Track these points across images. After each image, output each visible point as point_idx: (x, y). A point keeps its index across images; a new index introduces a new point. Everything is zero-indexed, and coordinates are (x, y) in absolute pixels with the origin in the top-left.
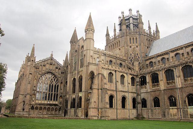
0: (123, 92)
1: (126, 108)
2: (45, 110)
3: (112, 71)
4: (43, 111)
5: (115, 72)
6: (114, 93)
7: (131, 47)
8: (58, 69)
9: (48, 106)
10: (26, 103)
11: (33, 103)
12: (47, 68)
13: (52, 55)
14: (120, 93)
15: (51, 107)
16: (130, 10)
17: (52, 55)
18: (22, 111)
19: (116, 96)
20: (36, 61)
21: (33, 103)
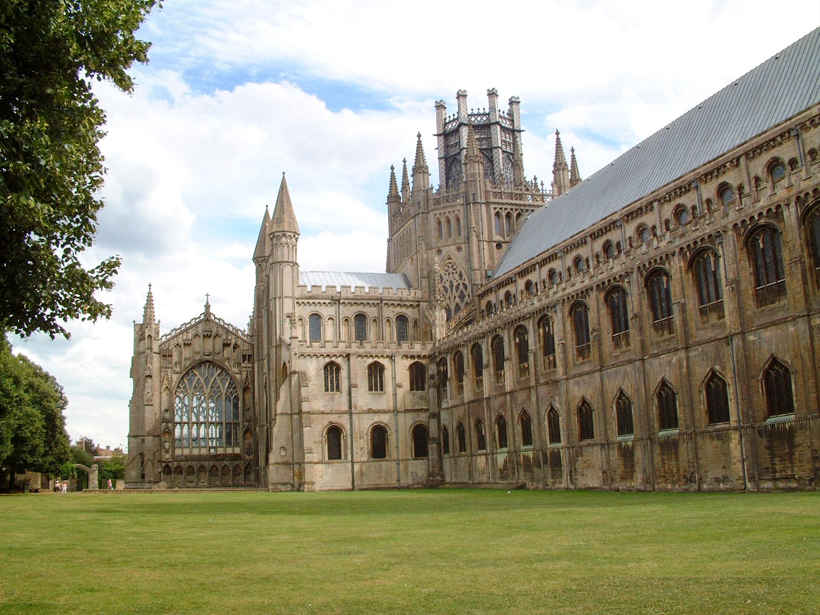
0: (378, 412)
1: (387, 458)
2: (202, 475)
3: (334, 359)
4: (198, 477)
5: (346, 359)
6: (344, 421)
7: (439, 252)
8: (232, 346)
9: (212, 463)
10: (146, 458)
11: (167, 456)
12: (197, 349)
13: (207, 307)
14: (366, 416)
15: (220, 465)
16: (461, 96)
17: (207, 307)
18: (140, 480)
19: (348, 427)
20: (161, 334)
21: (167, 456)
